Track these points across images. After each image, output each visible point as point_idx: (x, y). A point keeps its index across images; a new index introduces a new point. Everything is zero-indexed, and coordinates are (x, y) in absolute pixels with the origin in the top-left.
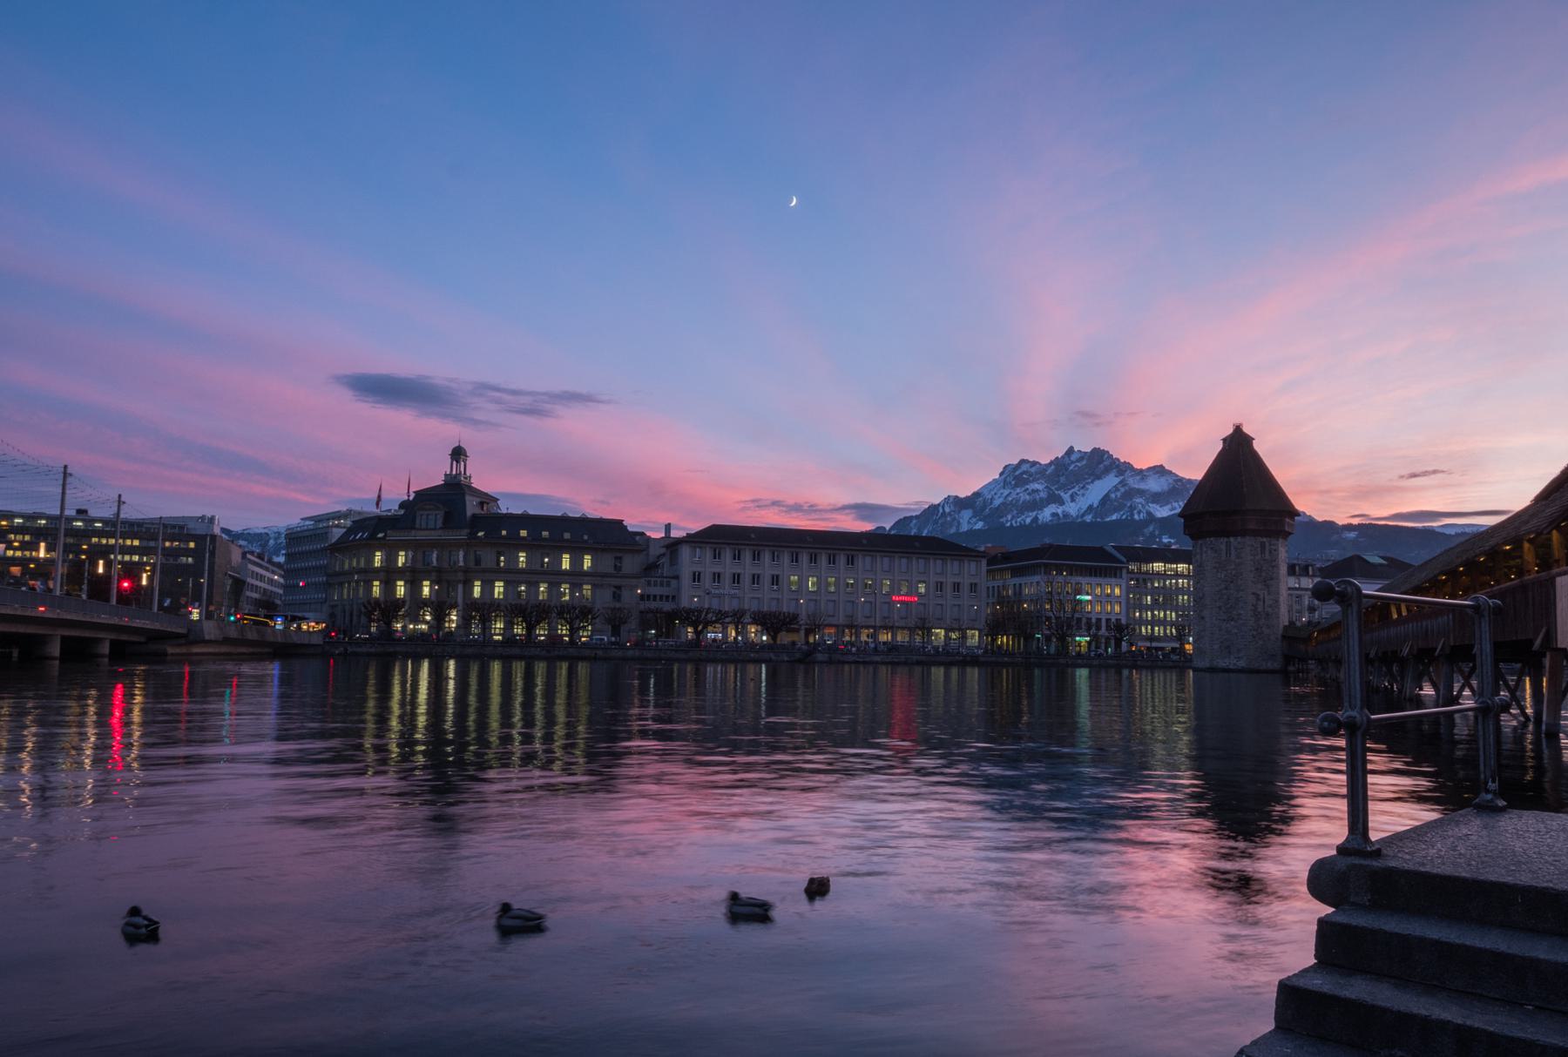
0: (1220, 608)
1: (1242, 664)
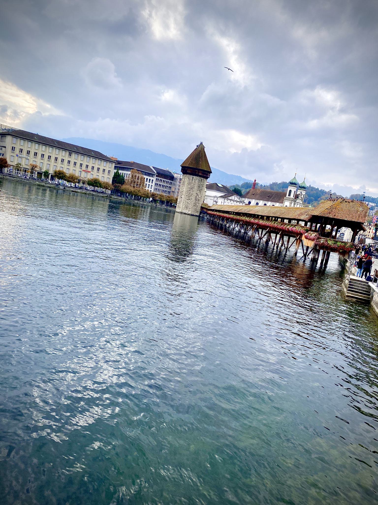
1: (190, 213)
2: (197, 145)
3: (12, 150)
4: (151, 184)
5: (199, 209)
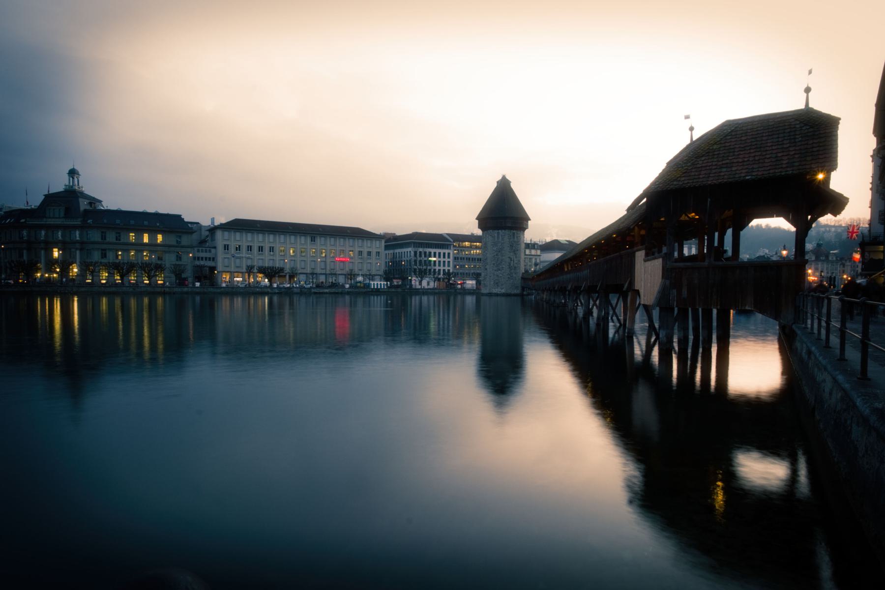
0: (494, 264)
1: (503, 291)
2: (497, 180)
3: (225, 250)
4: (447, 260)
5: (518, 282)
